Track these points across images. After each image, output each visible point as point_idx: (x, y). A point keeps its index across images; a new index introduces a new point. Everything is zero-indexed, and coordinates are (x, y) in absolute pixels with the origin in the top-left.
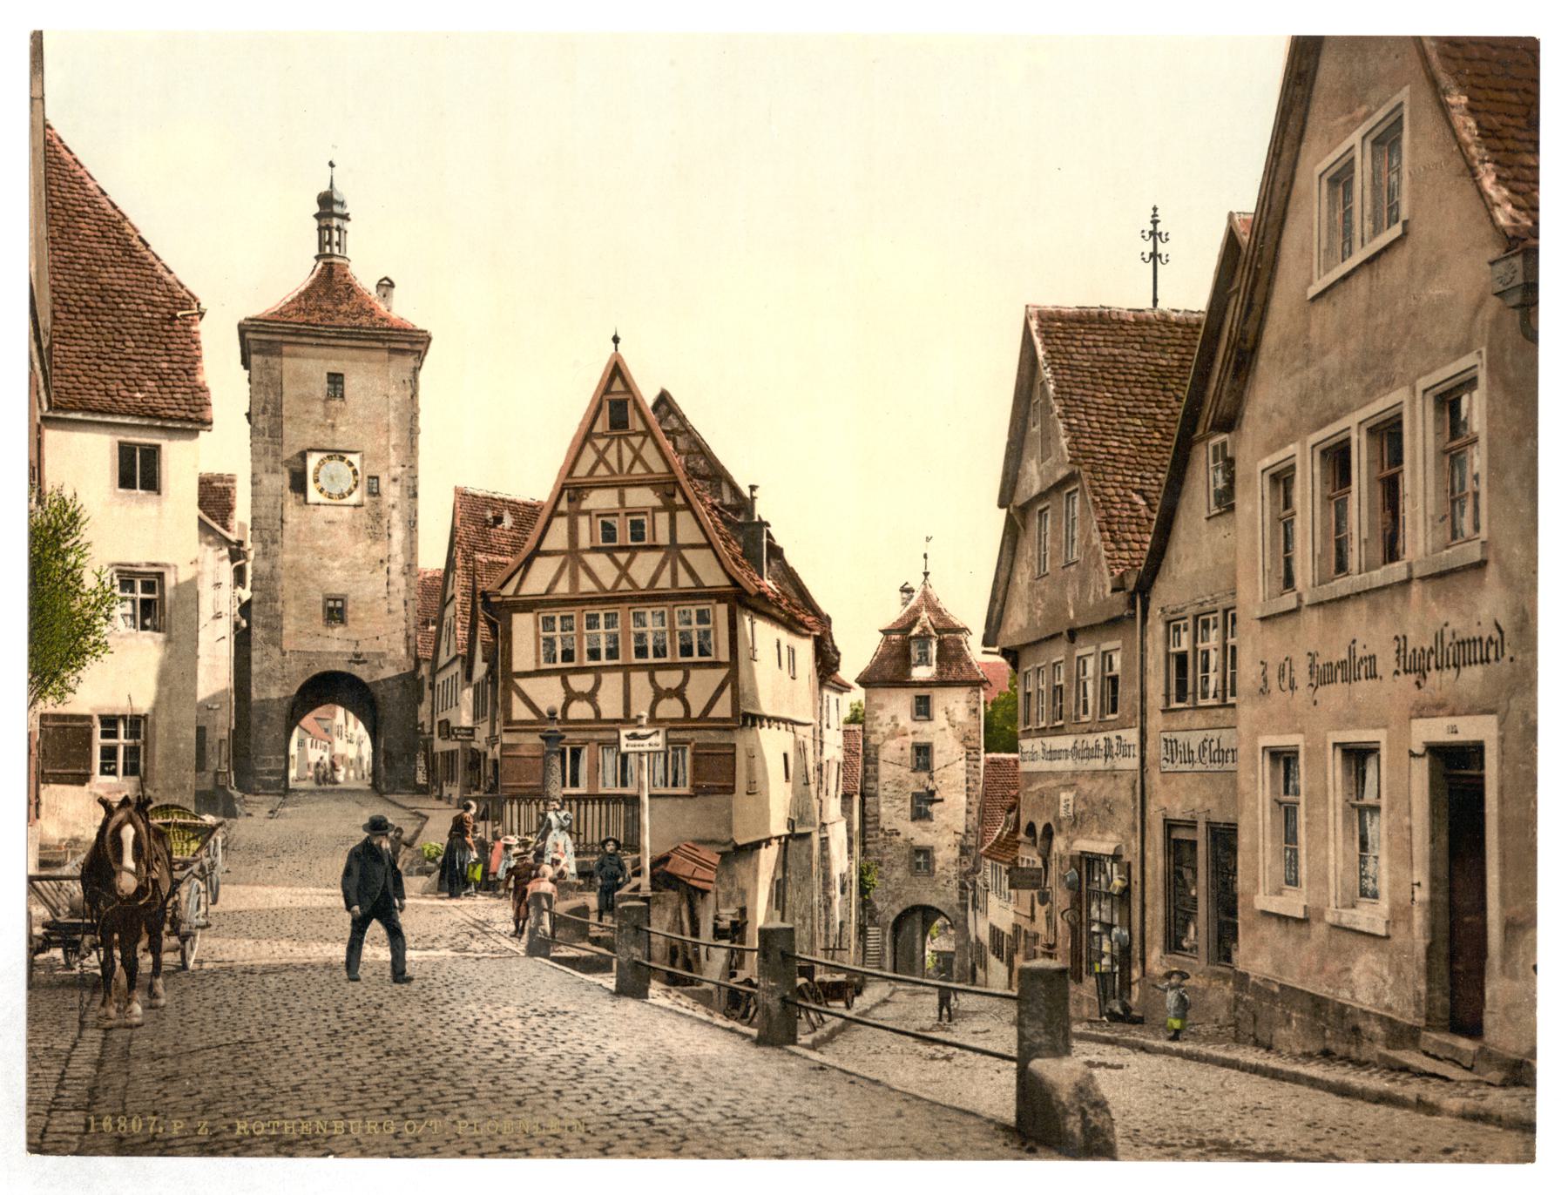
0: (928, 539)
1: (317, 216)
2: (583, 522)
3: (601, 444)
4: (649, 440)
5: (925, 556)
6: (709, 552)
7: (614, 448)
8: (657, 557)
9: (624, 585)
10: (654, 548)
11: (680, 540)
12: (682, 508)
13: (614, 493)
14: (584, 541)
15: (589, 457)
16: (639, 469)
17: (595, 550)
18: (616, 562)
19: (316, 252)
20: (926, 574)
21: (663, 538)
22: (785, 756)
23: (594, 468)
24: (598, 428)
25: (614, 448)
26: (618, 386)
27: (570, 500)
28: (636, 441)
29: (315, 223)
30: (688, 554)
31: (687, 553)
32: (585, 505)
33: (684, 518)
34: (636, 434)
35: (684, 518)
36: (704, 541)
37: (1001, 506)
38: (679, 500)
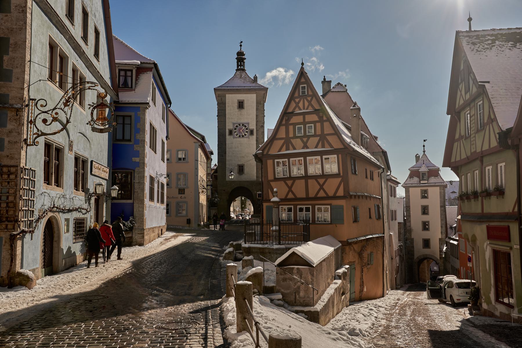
0: (425, 141)
2: (291, 128)
3: (297, 100)
4: (314, 98)
5: (424, 146)
6: (336, 137)
7: (302, 102)
10: (315, 135)
11: (325, 133)
12: (326, 121)
13: (302, 117)
14: (291, 135)
15: (293, 105)
16: (310, 110)
17: (295, 137)
20: (424, 152)
21: (319, 132)
22: (370, 209)
23: (295, 108)
24: (296, 95)
25: (302, 102)
26: (303, 80)
27: (286, 120)
28: (309, 99)
30: (328, 138)
31: (327, 137)
32: (290, 122)
33: (326, 124)
34: (310, 96)
35: (326, 124)
36: (334, 132)
37: (448, 114)
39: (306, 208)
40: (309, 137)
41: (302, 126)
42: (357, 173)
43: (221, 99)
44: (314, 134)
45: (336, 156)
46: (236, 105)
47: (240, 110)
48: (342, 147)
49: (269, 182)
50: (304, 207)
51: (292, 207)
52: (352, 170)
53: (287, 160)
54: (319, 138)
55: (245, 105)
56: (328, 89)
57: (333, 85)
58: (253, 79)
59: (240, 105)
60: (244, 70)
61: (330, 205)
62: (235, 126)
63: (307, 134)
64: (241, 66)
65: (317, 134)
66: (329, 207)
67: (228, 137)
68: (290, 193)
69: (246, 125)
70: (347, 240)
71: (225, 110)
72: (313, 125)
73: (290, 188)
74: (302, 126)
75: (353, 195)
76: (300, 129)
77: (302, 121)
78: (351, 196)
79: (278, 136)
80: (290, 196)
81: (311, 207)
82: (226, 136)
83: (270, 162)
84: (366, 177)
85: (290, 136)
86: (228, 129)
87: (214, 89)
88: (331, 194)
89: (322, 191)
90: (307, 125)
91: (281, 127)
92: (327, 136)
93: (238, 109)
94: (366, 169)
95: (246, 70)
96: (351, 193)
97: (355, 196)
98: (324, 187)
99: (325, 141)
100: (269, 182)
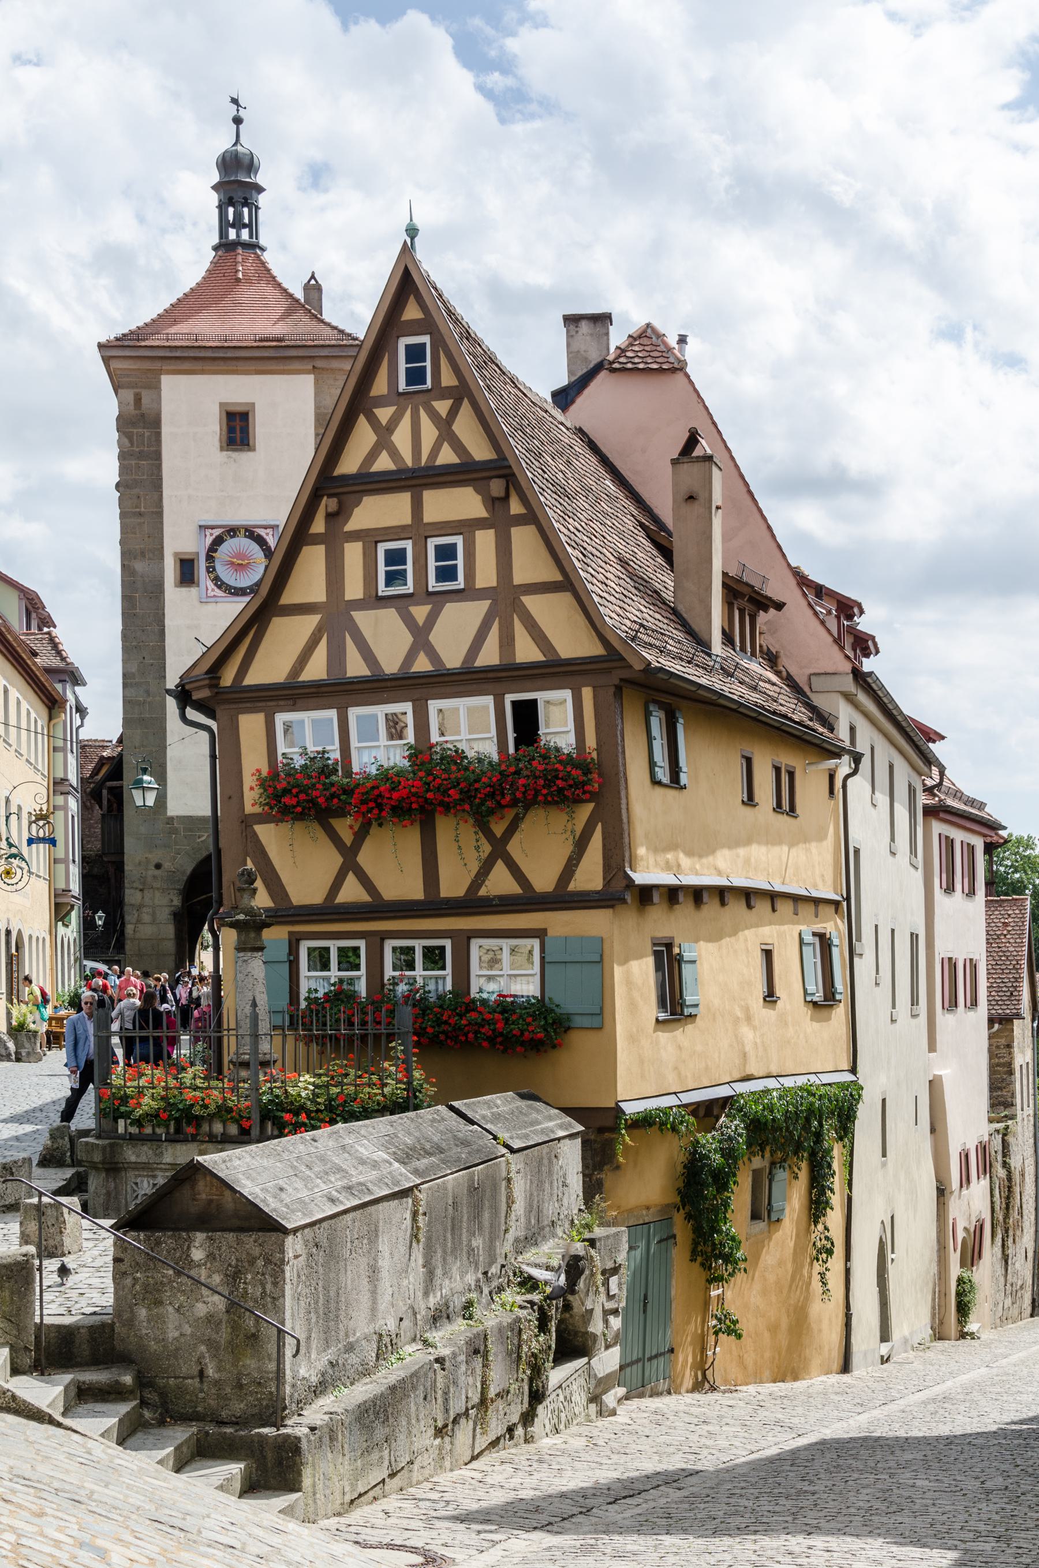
1: (215, 188)
2: (353, 553)
6: (565, 598)
8: (476, 610)
9: (422, 664)
11: (519, 578)
13: (404, 500)
14: (354, 589)
18: (409, 621)
19: (216, 240)
21: (486, 576)
29: (214, 198)
31: (527, 600)
33: (522, 537)
35: (522, 537)
36: (559, 577)
38: (516, 507)
39: (341, 950)
40: (438, 599)
41: (408, 545)
42: (684, 779)
43: (138, 400)
44: (462, 586)
45: (566, 695)
46: (214, 428)
47: (235, 455)
48: (598, 650)
49: (247, 822)
50: (418, 945)
51: (361, 944)
52: (652, 764)
53: (332, 714)
54: (487, 603)
55: (261, 429)
56: (594, 358)
57: (617, 338)
58: (299, 295)
59: (231, 430)
60: (253, 247)
61: (540, 934)
62: (209, 540)
63: (433, 584)
64: (238, 224)
65: (480, 584)
66: (536, 943)
67: (174, 596)
68: (351, 879)
69: (262, 532)
70: (617, 1104)
71: (157, 456)
72: (459, 540)
73: (349, 854)
74: (408, 545)
75: (657, 887)
76: (396, 557)
77: (407, 519)
78: (645, 894)
79: (289, 597)
80: (351, 892)
81: (447, 944)
82: (162, 591)
83: (251, 725)
84: (750, 800)
85: (348, 597)
86: (176, 554)
87: (101, 346)
88: (544, 881)
89: (500, 868)
90: (432, 543)
91: (305, 548)
92: (523, 598)
93: (222, 449)
94: (749, 761)
95: (263, 249)
96: (640, 877)
97: (672, 894)
98: (510, 848)
99: (515, 616)
100: (247, 822)
